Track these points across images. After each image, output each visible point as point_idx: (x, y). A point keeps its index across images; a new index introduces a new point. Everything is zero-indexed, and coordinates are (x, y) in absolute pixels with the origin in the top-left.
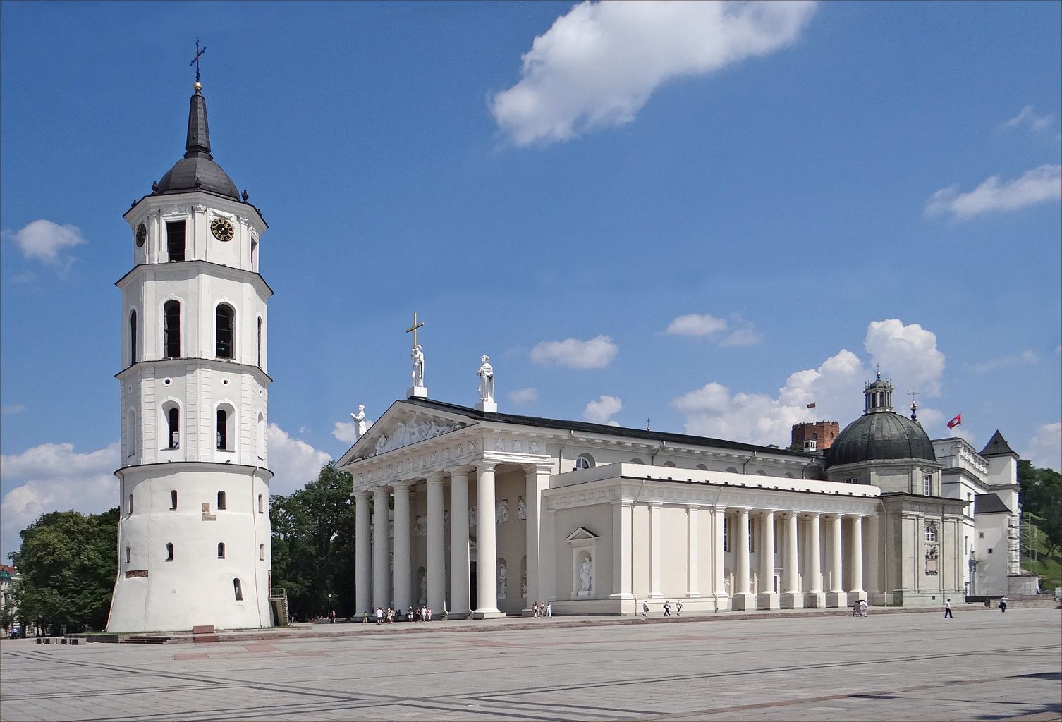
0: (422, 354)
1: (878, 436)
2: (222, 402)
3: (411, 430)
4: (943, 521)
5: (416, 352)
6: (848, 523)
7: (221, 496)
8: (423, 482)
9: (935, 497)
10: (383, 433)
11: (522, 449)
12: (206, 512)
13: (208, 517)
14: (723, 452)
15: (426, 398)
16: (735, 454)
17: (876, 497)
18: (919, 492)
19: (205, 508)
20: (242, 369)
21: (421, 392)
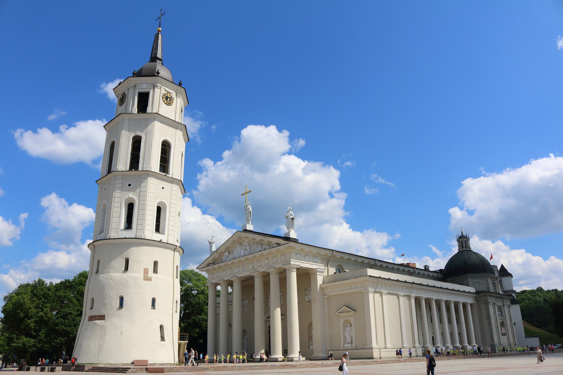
0: (250, 207)
2: (160, 200)
3: (246, 248)
4: (504, 306)
5: (247, 206)
6: (464, 305)
7: (156, 263)
8: (251, 278)
9: (498, 294)
10: (227, 250)
11: (309, 259)
12: (146, 275)
13: (147, 279)
17: (474, 293)
18: (492, 291)
19: (146, 271)
20: (173, 181)
21: (250, 227)
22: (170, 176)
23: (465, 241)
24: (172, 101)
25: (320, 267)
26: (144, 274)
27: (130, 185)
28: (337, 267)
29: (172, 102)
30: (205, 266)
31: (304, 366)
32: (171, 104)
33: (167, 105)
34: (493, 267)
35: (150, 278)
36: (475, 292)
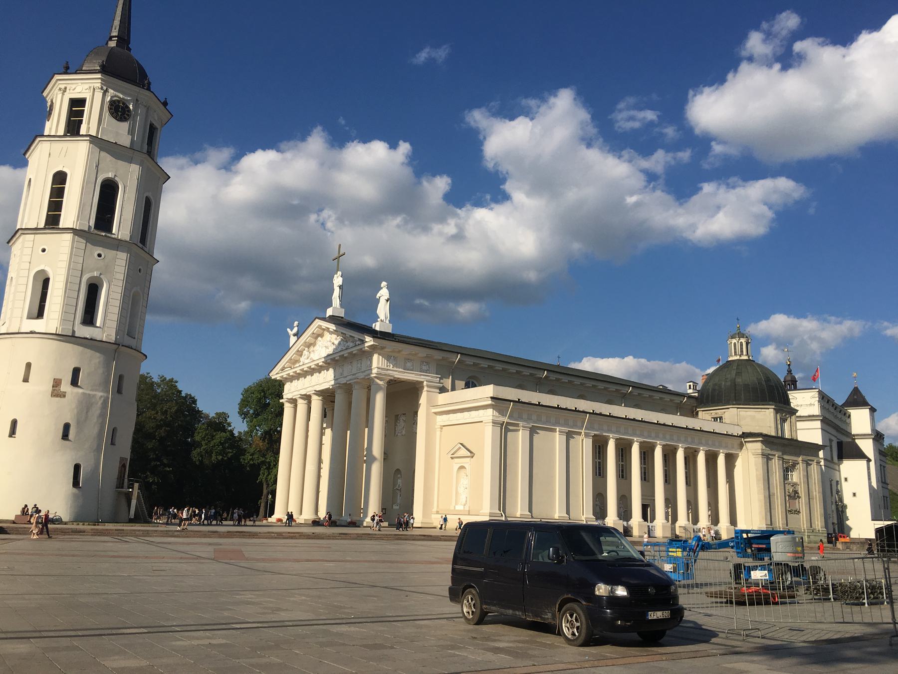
1: (739, 380)
12: (57, 388)
14: (601, 386)
15: (342, 318)
16: (613, 388)
19: (57, 383)
20: (117, 245)
22: (113, 236)
23: (741, 342)
24: (127, 113)
25: (432, 379)
26: (53, 387)
27: (44, 250)
28: (471, 380)
29: (128, 115)
30: (279, 371)
31: (273, 535)
32: (124, 117)
33: (118, 120)
34: (788, 392)
35: (63, 393)
36: (740, 433)
